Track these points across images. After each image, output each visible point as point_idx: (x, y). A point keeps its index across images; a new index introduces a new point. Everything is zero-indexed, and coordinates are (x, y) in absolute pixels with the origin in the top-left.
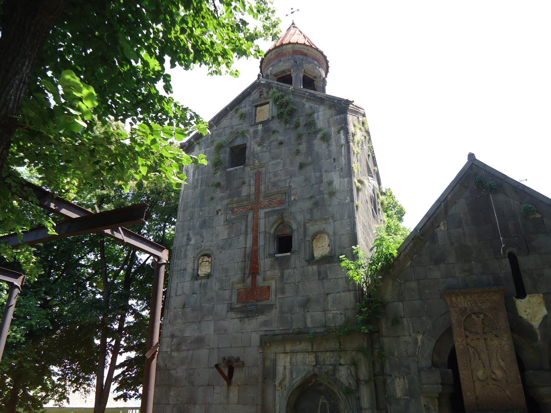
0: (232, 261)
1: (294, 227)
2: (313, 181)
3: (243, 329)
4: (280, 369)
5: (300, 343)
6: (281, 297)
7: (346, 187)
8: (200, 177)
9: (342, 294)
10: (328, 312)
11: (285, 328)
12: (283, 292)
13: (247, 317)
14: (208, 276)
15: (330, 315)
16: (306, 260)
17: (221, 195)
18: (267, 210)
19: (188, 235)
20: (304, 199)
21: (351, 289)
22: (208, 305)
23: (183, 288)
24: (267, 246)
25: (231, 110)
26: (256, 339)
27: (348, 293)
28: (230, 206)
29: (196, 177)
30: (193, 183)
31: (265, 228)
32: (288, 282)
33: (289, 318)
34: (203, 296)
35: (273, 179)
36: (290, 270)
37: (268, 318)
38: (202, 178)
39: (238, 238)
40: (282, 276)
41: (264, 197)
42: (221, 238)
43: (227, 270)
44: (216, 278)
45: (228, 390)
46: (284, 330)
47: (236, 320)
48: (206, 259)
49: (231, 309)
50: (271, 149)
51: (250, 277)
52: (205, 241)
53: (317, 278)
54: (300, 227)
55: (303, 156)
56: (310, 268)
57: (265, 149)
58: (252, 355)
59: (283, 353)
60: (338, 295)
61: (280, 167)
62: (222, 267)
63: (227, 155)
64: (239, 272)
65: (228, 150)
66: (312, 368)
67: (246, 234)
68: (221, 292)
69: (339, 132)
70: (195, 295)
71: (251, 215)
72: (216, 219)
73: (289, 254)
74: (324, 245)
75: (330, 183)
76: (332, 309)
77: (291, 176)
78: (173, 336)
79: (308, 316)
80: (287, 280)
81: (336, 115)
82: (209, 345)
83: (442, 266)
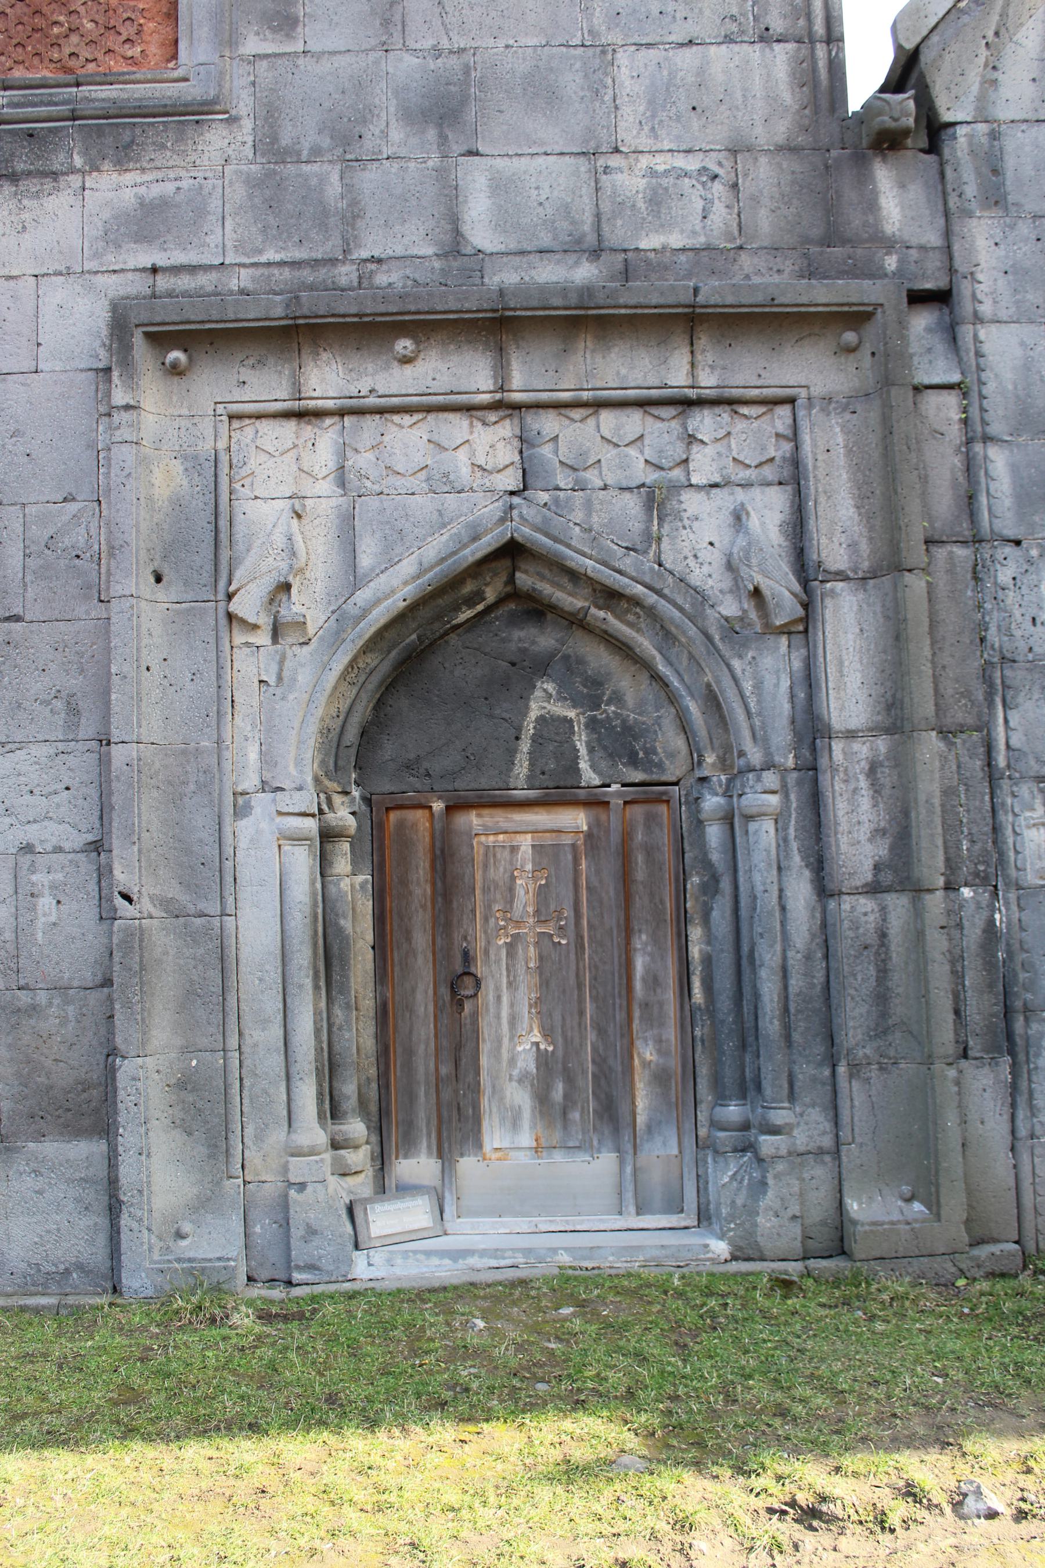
4: (261, 516)
6: (269, 48)
9: (719, 54)
10: (615, 161)
11: (299, 254)
15: (629, 181)
21: (778, 25)
26: (76, 320)
27: (755, 53)
33: (334, 187)
37: (170, 187)
46: (295, 264)
59: (287, 415)
60: (687, 58)
66: (489, 509)
76: (644, 142)
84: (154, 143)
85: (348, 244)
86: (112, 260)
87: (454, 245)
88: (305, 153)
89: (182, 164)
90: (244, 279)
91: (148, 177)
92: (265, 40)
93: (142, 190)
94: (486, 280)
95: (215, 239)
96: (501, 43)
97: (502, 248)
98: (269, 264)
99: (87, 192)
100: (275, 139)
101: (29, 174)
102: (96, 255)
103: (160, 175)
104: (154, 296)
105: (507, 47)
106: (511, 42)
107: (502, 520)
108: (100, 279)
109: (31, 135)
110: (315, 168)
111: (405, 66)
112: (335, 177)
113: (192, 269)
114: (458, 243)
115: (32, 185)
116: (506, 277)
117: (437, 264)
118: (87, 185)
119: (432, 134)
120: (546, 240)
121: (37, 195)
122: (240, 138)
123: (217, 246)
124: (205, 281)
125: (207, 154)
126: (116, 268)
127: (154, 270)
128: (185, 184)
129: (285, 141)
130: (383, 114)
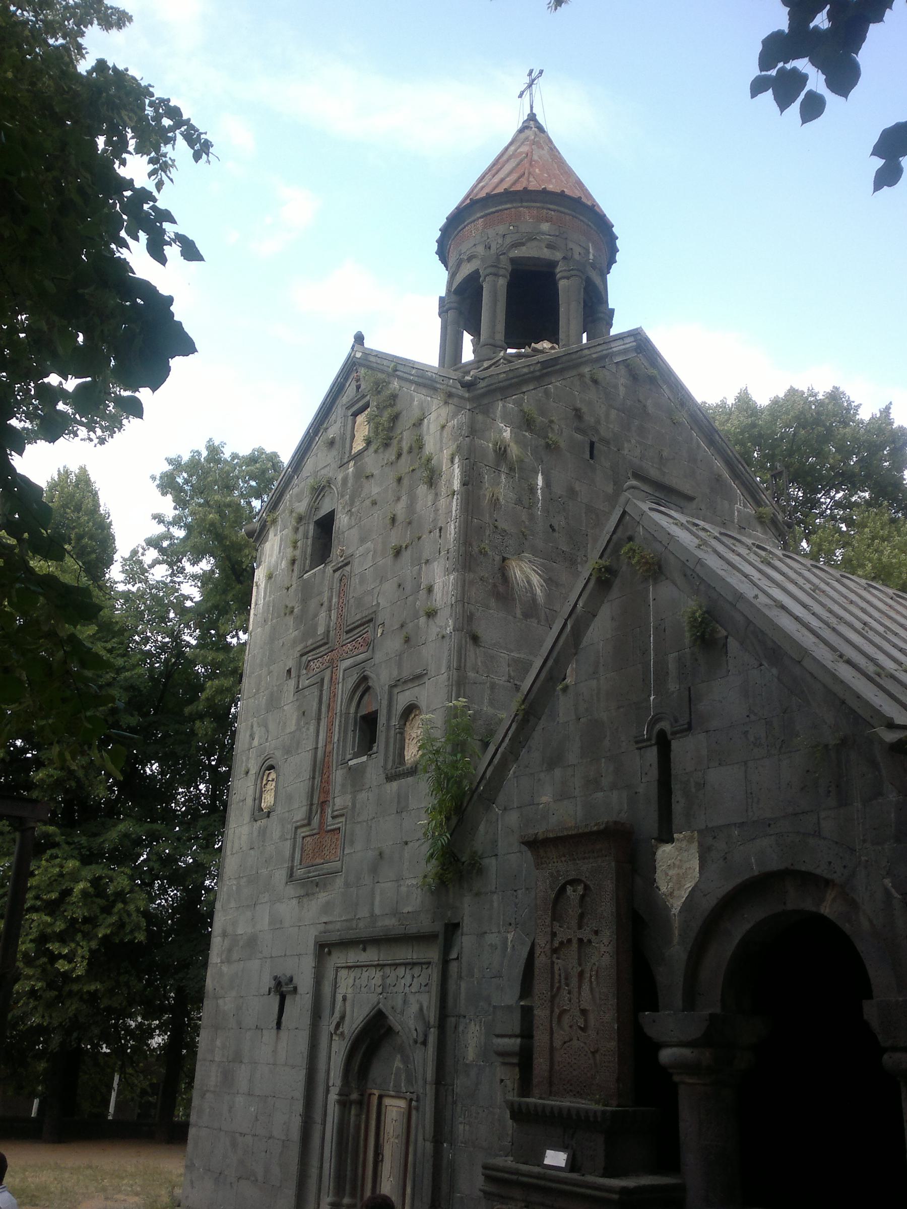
2: (409, 587)
5: (364, 950)
7: (450, 596)
12: (352, 843)
13: (307, 895)
17: (293, 635)
19: (252, 726)
23: (240, 838)
25: (316, 433)
29: (267, 599)
30: (263, 613)
42: (288, 731)
45: (278, 1038)
52: (269, 739)
58: (304, 974)
63: (310, 542)
64: (305, 803)
65: (312, 527)
67: (319, 720)
69: (452, 461)
70: (252, 852)
73: (364, 758)
75: (430, 590)
78: (224, 935)
81: (453, 417)
82: (261, 952)
83: (558, 772)
87: (372, 915)
107: (378, 1003)
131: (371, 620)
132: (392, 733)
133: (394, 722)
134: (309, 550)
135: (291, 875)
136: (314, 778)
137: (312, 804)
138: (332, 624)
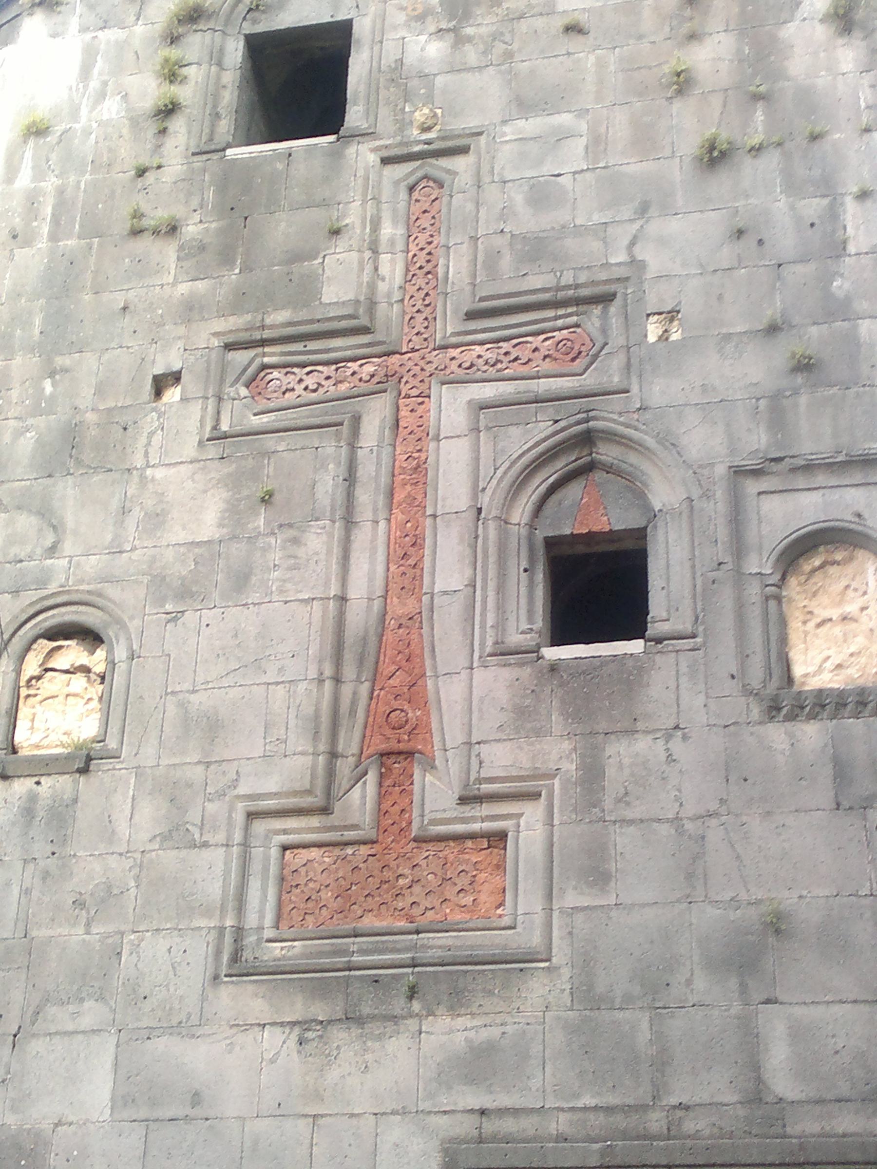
0: (247, 680)
1: (663, 494)
2: (785, 239)
3: (318, 1097)
6: (585, 901)
8: (50, 184)
11: (612, 1099)
12: (597, 873)
13: (352, 1019)
14: (83, 762)
16: (748, 692)
17: (184, 288)
18: (488, 391)
20: (728, 337)
22: (74, 935)
24: (478, 594)
28: (241, 357)
31: (476, 491)
32: (629, 814)
33: (644, 1033)
34: (46, 875)
35: (528, 221)
36: (642, 744)
37: (496, 1032)
38: (60, 192)
39: (296, 541)
40: (592, 775)
41: (471, 316)
43: (212, 727)
44: (139, 771)
46: (609, 1110)
47: (272, 1039)
48: (73, 653)
49: (238, 963)
50: (509, 55)
51: (371, 778)
52: (68, 547)
53: (824, 795)
54: (707, 495)
55: (716, 102)
56: (777, 734)
57: (471, 55)
61: (574, 155)
62: (182, 705)
64: (298, 742)
68: (170, 858)
71: (376, 415)
72: (151, 420)
73: (636, 646)
74: (851, 608)
77: (643, 210)
79: (775, 1027)
80: (623, 799)
84: (484, 990)
85: (658, 1091)
86: (445, 1101)
87: (756, 1095)
88: (618, 1000)
89: (509, 1010)
90: (560, 1124)
91: (476, 1022)
92: (582, 894)
93: (472, 1034)
94: (788, 1130)
95: (535, 1083)
96: (795, 894)
97: (802, 1096)
98: (585, 1109)
99: (423, 1035)
100: (591, 987)
101: (373, 1017)
102: (431, 1096)
103: (487, 1020)
104: (481, 1140)
105: (801, 897)
106: (805, 893)
108: (434, 1120)
109: (376, 981)
110: (627, 1014)
111: (707, 917)
112: (645, 1025)
113: (515, 1112)
114: (759, 1092)
115: (374, 1028)
116: (806, 1125)
117: (741, 1112)
118: (424, 1029)
119: (733, 983)
120: (844, 1089)
121: (380, 1038)
122: (558, 986)
123: (537, 1090)
124: (527, 1125)
125: (530, 1002)
126: (448, 1109)
127: (483, 1112)
128: (509, 1029)
129: (600, 988)
130: (688, 963)
131: (606, 299)
132: (754, 592)
133: (760, 564)
134: (229, 97)
135: (235, 958)
136: (337, 680)
137: (333, 755)
138: (382, 287)
